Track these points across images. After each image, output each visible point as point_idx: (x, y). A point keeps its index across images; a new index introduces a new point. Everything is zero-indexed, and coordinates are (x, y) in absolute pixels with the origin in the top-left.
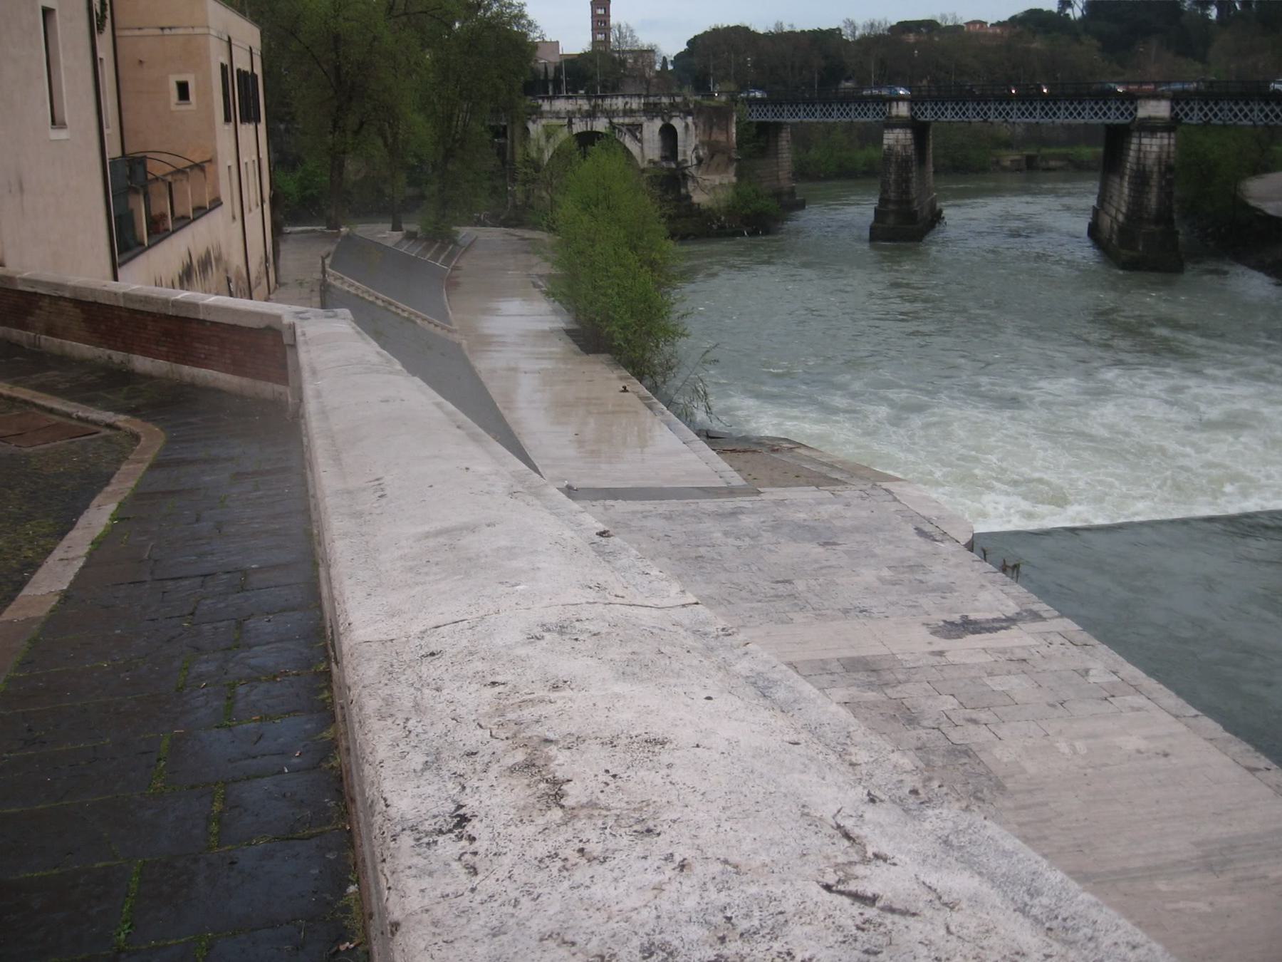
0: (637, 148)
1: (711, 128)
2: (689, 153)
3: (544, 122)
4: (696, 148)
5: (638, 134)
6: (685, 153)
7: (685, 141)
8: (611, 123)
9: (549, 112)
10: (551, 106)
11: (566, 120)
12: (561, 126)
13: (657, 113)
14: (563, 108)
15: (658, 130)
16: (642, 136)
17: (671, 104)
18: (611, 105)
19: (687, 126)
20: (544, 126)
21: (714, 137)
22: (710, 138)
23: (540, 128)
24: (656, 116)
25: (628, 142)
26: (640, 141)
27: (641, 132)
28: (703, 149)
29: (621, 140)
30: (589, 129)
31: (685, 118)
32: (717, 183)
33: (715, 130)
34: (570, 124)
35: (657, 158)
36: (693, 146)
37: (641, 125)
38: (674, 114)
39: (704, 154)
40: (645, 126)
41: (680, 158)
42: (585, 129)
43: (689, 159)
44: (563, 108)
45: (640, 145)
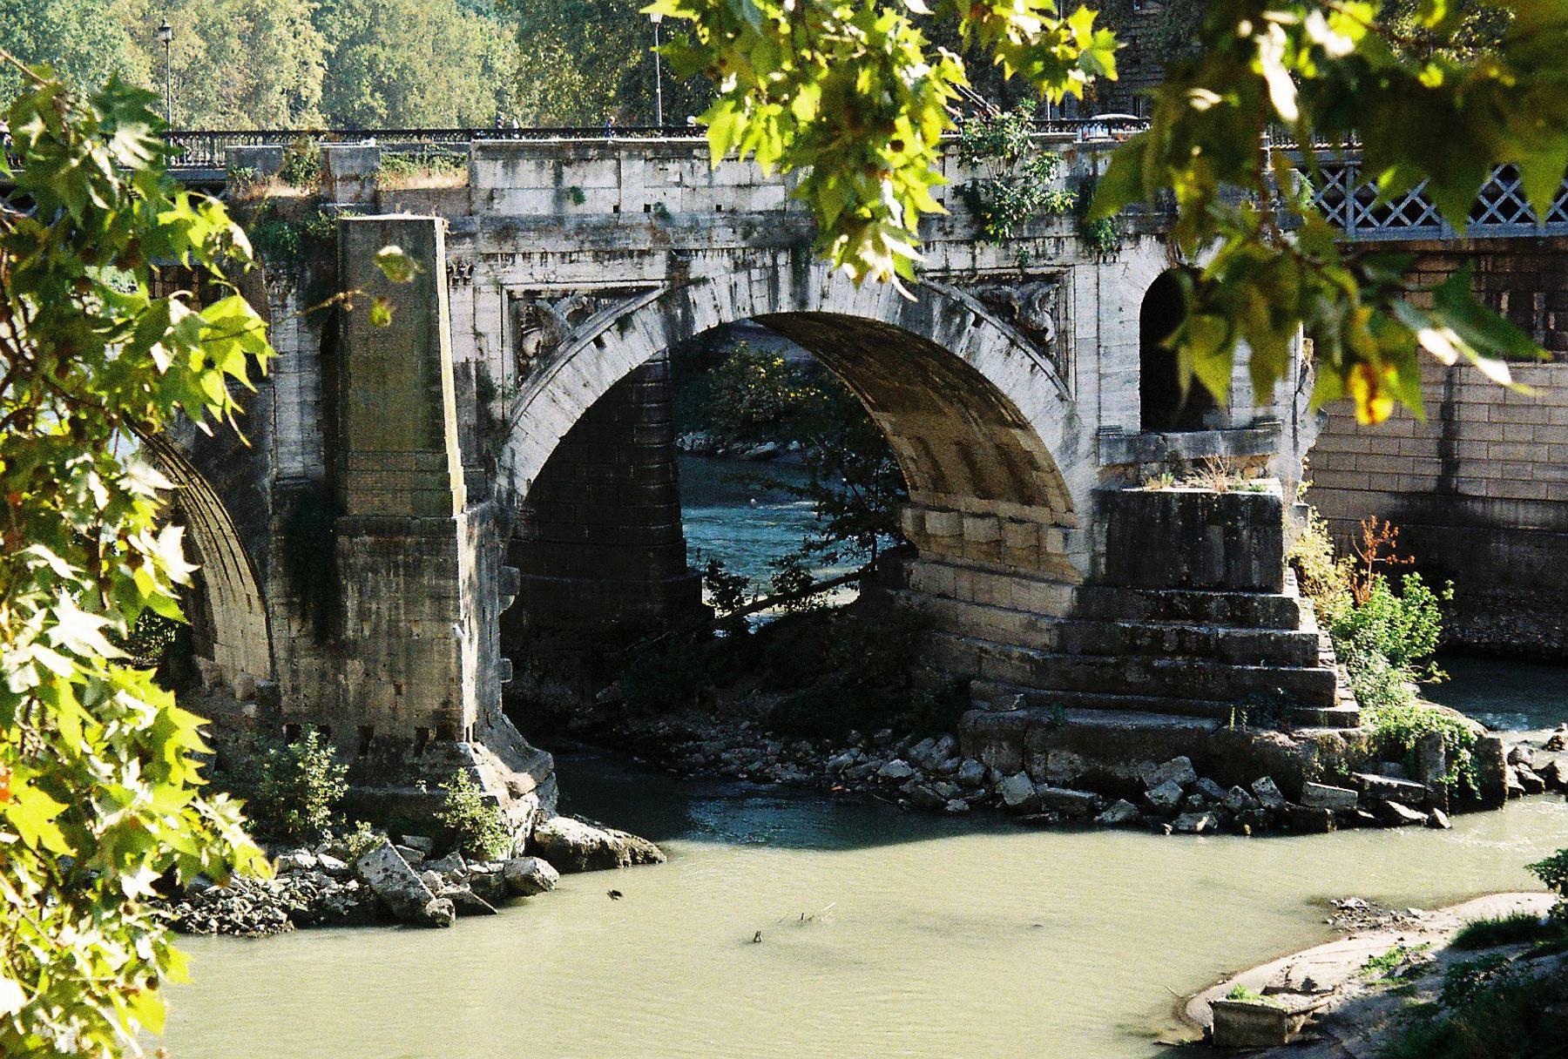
0: (1041, 379)
11: (655, 270)
23: (492, 314)
30: (786, 306)
34: (680, 283)
40: (1083, 277)
42: (762, 308)
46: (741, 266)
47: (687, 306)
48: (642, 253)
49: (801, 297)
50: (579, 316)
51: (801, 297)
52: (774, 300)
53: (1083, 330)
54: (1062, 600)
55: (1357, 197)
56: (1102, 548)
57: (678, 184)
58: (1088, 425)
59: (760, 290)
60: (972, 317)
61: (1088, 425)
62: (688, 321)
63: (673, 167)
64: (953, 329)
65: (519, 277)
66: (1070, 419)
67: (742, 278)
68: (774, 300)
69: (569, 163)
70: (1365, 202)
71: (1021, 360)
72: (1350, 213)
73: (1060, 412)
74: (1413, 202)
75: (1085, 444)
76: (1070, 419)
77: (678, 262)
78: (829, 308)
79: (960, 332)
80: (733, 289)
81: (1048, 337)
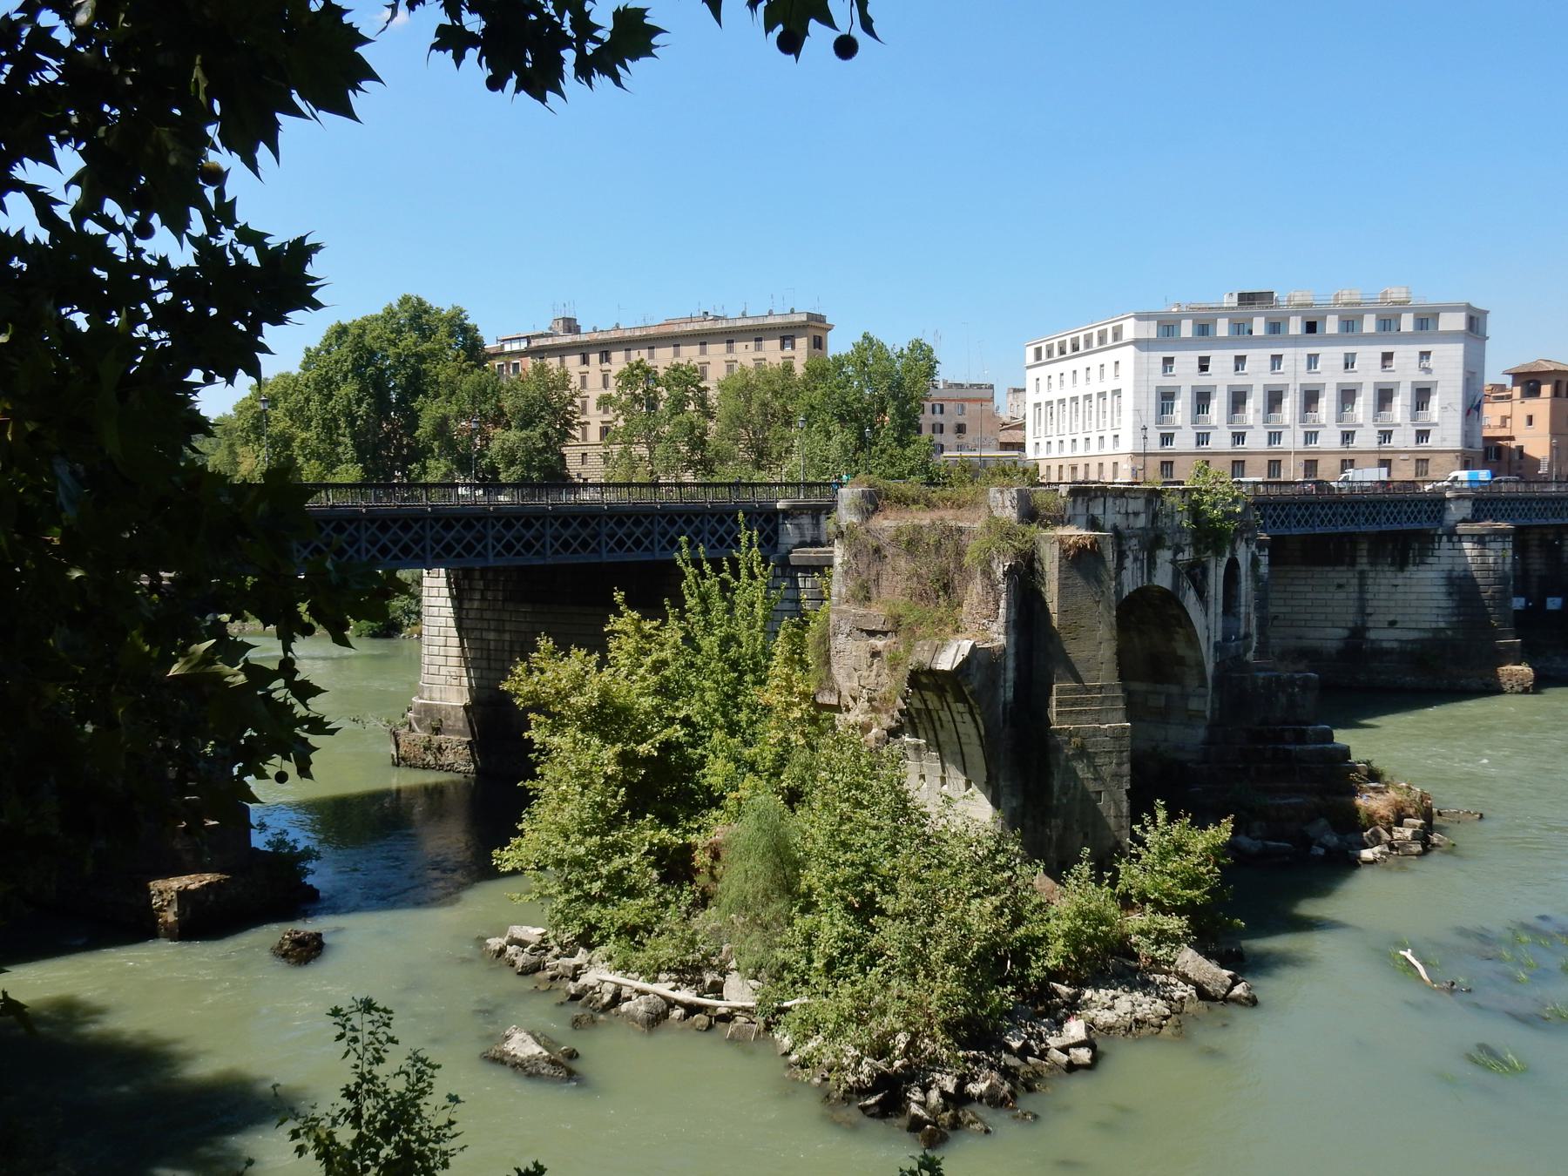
8: (1174, 562)
25: (1190, 600)
40: (1212, 565)
42: (1140, 585)
46: (1136, 559)
49: (1150, 580)
51: (1150, 580)
53: (1212, 592)
54: (1201, 733)
55: (369, 542)
56: (1217, 706)
57: (1119, 512)
58: (1212, 640)
62: (1122, 590)
68: (1143, 583)
70: (499, 541)
71: (1198, 607)
72: (603, 544)
74: (384, 544)
75: (1212, 650)
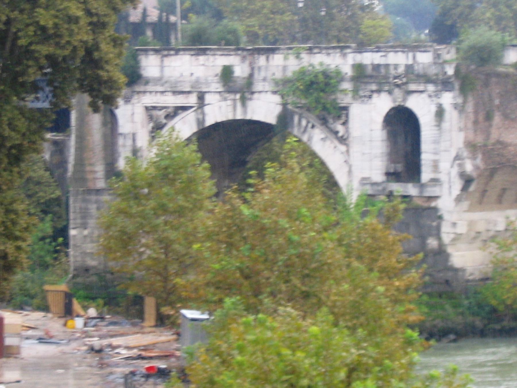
1: (489, 117)
2: (445, 165)
3: (149, 100)
4: (457, 157)
5: (340, 129)
6: (435, 166)
7: (436, 142)
9: (159, 80)
10: (162, 67)
11: (192, 100)
12: (184, 108)
13: (380, 84)
14: (187, 74)
15: (380, 119)
16: (347, 131)
17: (409, 68)
18: (285, 68)
19: (440, 113)
20: (147, 108)
21: (495, 135)
22: (488, 136)
24: (379, 91)
26: (343, 140)
27: (345, 123)
28: (474, 158)
29: (305, 138)
30: (239, 116)
31: (437, 94)
32: (501, 227)
33: (497, 119)
35: (378, 177)
36: (453, 154)
37: (346, 109)
38: (412, 87)
39: (477, 168)
41: (426, 176)
42: (230, 117)
43: (443, 177)
44: (187, 74)
45: (343, 148)
47: (203, 114)
48: (189, 92)
50: (169, 117)
52: (235, 114)
57: (203, 65)
59: (230, 109)
60: (310, 125)
61: (358, 175)
62: (204, 121)
63: (202, 58)
64: (302, 130)
65: (149, 100)
66: (350, 172)
67: (223, 104)
69: (166, 56)
73: (346, 169)
76: (350, 172)
77: (201, 97)
78: (256, 118)
79: (305, 131)
80: (220, 107)
81: (340, 134)
